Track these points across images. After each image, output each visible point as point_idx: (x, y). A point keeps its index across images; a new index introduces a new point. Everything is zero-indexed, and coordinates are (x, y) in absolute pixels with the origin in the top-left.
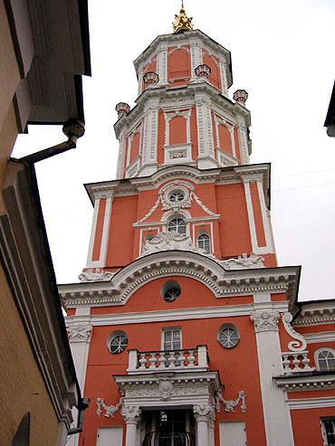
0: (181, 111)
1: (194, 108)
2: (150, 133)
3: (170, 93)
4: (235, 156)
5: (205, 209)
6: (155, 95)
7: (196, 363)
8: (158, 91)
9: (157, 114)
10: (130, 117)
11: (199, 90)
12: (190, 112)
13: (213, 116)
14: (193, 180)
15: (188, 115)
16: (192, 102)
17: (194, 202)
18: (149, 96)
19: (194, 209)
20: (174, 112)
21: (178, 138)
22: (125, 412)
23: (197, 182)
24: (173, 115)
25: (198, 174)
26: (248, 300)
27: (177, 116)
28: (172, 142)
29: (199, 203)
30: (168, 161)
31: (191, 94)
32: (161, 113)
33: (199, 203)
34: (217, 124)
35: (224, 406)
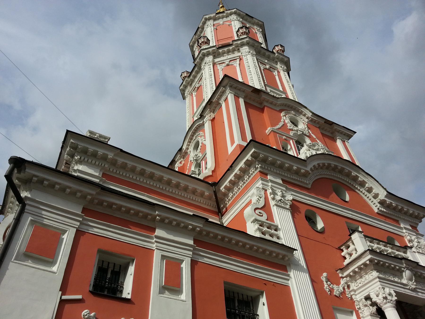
2: (208, 80)
3: (220, 51)
4: (281, 89)
6: (208, 54)
8: (210, 50)
9: (212, 66)
10: (191, 77)
11: (242, 45)
13: (258, 63)
16: (239, 54)
18: (204, 55)
20: (224, 63)
24: (224, 65)
27: (228, 65)
31: (238, 48)
32: (214, 64)
34: (262, 68)
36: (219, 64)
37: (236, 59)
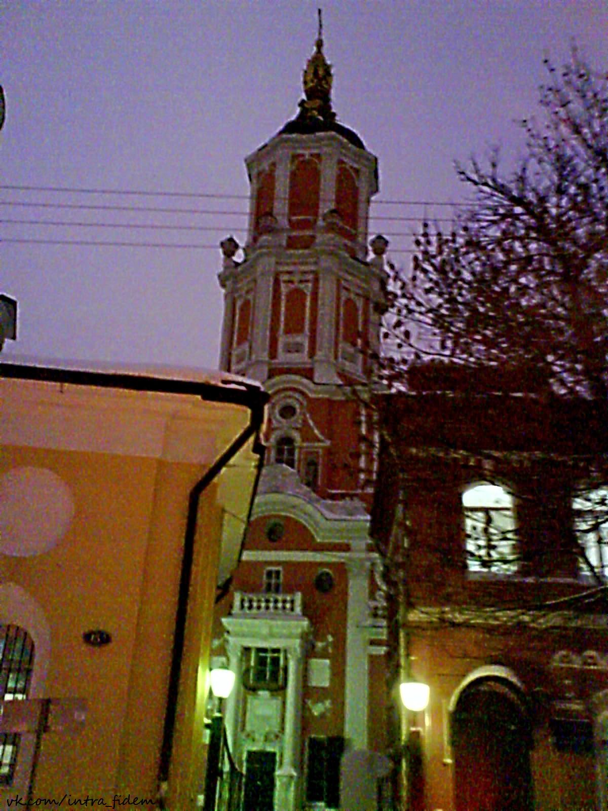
0: (301, 282)
1: (316, 281)
5: (316, 432)
7: (292, 609)
12: (310, 285)
14: (307, 391)
15: (308, 288)
17: (305, 422)
19: (305, 431)
20: (291, 282)
21: (294, 327)
22: (229, 648)
23: (311, 395)
25: (312, 386)
26: (346, 548)
28: (288, 332)
29: (311, 423)
30: (283, 357)
32: (277, 282)
33: (311, 423)
35: (313, 646)
36: (285, 282)
37: (307, 281)
